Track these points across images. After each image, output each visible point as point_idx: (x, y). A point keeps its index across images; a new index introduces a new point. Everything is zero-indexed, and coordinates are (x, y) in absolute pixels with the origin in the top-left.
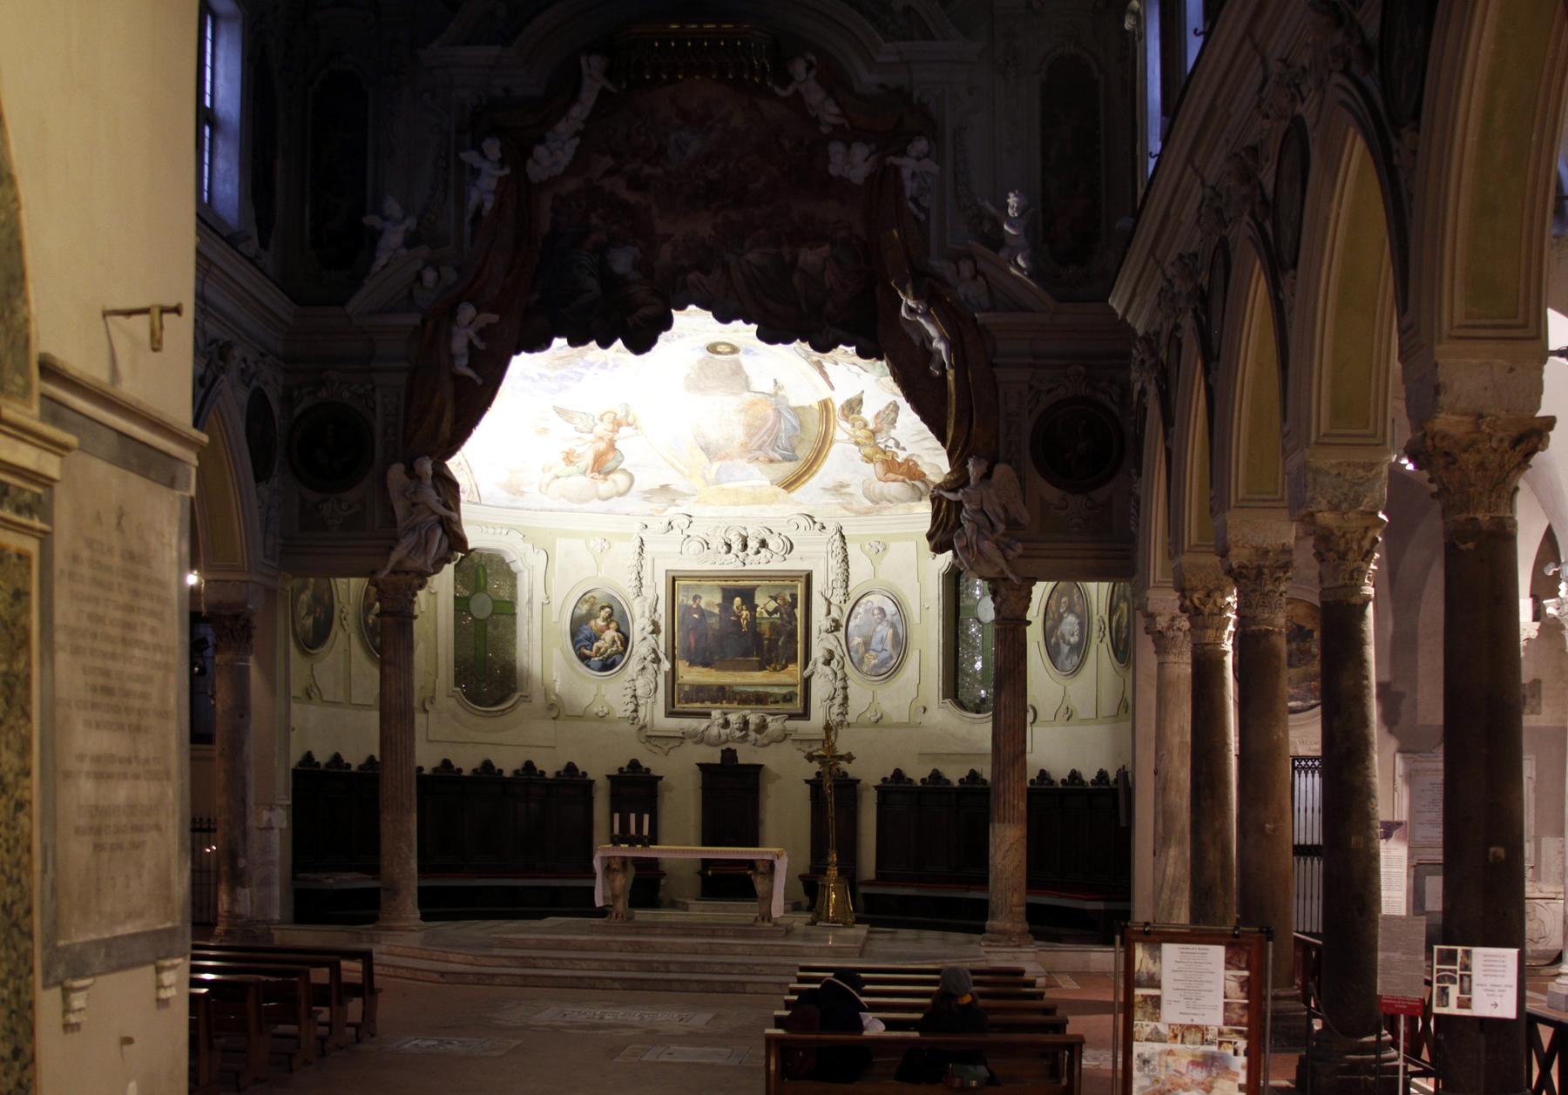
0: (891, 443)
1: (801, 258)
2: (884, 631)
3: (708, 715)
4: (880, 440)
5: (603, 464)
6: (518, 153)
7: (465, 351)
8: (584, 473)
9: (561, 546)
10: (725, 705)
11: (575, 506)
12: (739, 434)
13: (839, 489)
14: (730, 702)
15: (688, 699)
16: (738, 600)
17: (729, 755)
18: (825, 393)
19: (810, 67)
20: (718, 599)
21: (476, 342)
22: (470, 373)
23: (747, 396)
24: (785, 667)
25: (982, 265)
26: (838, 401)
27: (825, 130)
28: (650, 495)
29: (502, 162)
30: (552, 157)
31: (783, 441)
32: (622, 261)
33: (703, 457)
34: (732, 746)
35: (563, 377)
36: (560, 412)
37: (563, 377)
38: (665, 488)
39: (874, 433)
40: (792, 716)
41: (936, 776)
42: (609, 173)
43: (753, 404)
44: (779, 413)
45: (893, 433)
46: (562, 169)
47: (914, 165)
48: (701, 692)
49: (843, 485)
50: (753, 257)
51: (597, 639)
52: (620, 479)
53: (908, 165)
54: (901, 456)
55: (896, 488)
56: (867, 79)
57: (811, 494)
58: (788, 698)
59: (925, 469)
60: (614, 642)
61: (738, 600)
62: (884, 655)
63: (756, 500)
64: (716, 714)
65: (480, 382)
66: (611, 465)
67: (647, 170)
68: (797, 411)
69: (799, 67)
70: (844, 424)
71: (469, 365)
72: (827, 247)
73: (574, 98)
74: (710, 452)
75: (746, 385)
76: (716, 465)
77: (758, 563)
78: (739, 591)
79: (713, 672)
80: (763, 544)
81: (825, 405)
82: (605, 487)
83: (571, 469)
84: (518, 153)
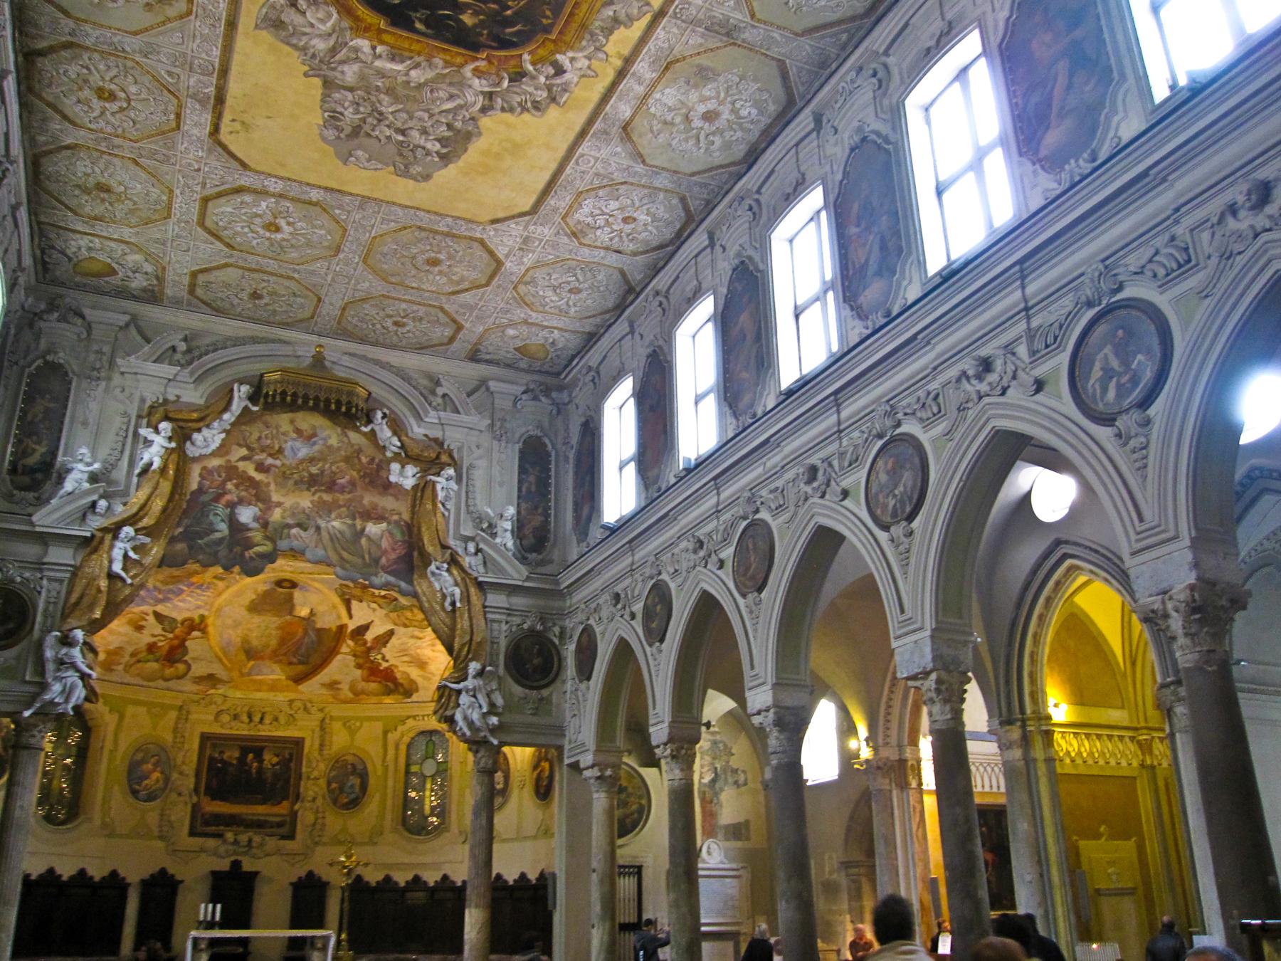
0: (379, 657)
1: (367, 529)
2: (355, 781)
3: (219, 836)
4: (373, 656)
5: (175, 654)
6: (182, 435)
7: (120, 558)
8: (157, 661)
9: (130, 710)
10: (235, 828)
11: (145, 683)
12: (274, 643)
13: (333, 685)
14: (238, 825)
15: (207, 823)
16: (251, 756)
17: (236, 864)
18: (345, 620)
19: (384, 416)
20: (237, 754)
21: (131, 554)
22: (123, 574)
23: (288, 617)
24: (279, 803)
25: (482, 546)
26: (352, 625)
27: (389, 454)
28: (199, 680)
29: (170, 439)
30: (208, 439)
31: (303, 650)
32: (246, 515)
33: (243, 657)
34: (239, 858)
35: (170, 591)
36: (158, 616)
37: (170, 591)
38: (211, 677)
39: (369, 650)
40: (283, 837)
41: (388, 879)
42: (244, 459)
43: (290, 624)
44: (306, 633)
45: (384, 650)
46: (209, 451)
47: (444, 483)
48: (218, 819)
49: (336, 683)
50: (336, 524)
51: (147, 778)
52: (181, 667)
53: (441, 482)
54: (385, 665)
55: (373, 686)
56: (417, 430)
57: (312, 687)
58: (280, 825)
59: (398, 675)
60: (158, 781)
61: (251, 756)
62: (353, 796)
63: (273, 687)
64: (230, 836)
65: (129, 581)
66: (177, 657)
67: (270, 461)
68: (320, 631)
69: (379, 414)
70: (350, 643)
71: (124, 569)
72: (384, 525)
73: (227, 408)
74: (251, 653)
75: (291, 610)
76: (252, 663)
77: (266, 731)
78: (253, 747)
79: (228, 805)
80: (276, 719)
81: (342, 628)
82: (169, 672)
83: (151, 657)
84: (182, 435)
